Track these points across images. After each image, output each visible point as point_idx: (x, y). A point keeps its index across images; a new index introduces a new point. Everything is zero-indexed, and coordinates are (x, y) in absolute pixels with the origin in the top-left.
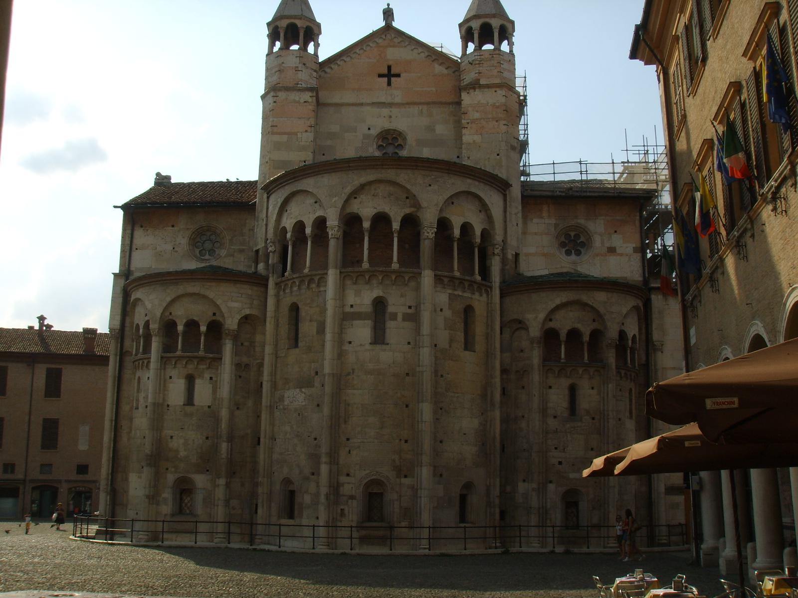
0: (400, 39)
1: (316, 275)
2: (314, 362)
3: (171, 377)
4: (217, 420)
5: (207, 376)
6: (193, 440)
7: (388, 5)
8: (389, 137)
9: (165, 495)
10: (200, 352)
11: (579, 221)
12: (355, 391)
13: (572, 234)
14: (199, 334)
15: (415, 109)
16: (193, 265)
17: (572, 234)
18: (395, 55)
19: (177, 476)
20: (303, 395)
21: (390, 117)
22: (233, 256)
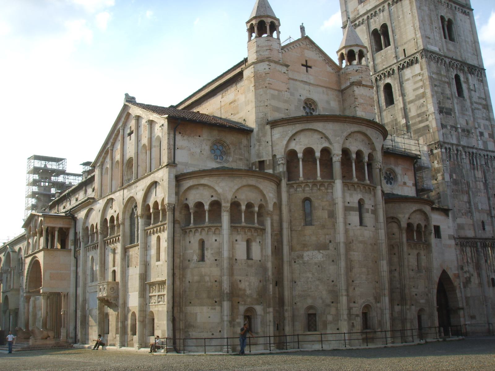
0: (311, 46)
1: (325, 182)
2: (328, 235)
3: (236, 240)
4: (265, 269)
5: (258, 240)
6: (254, 283)
7: (302, 24)
8: (308, 103)
9: (238, 320)
10: (205, 224)
11: (392, 166)
12: (355, 253)
13: (388, 173)
14: (240, 211)
15: (320, 89)
16: (212, 165)
17: (388, 173)
18: (310, 55)
19: (246, 307)
20: (321, 254)
21: (310, 91)
22: (236, 162)
